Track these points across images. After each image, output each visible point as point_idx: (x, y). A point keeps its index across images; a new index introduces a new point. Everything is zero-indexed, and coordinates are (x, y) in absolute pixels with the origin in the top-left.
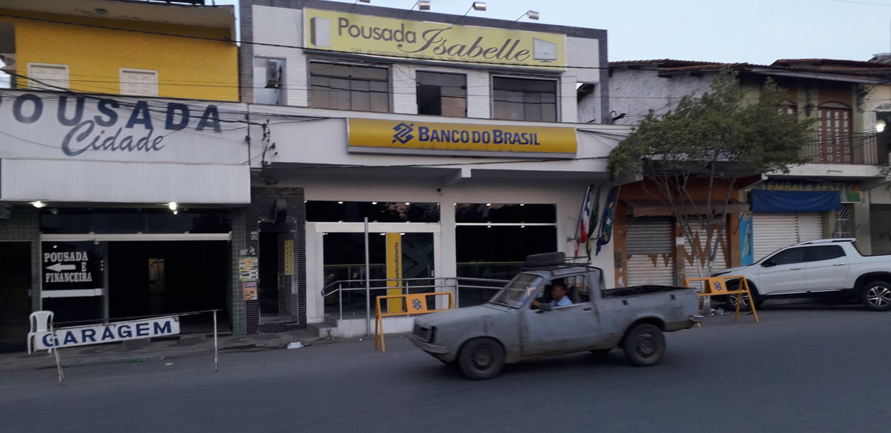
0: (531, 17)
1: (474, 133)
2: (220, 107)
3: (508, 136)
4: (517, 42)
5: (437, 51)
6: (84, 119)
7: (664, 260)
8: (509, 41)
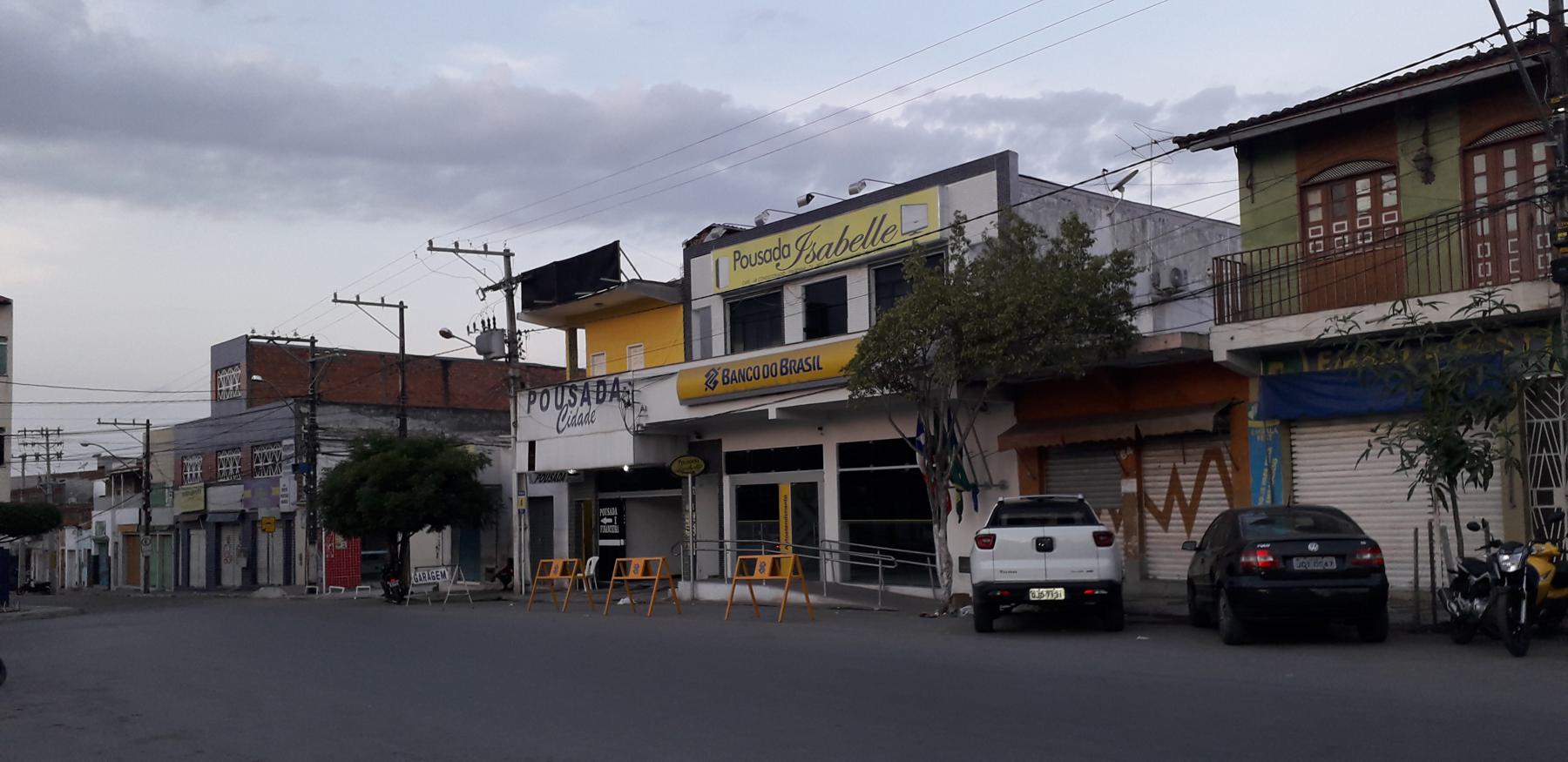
0: (851, 193)
1: (764, 366)
2: (621, 378)
3: (793, 364)
4: (884, 216)
5: (809, 260)
6: (564, 404)
7: (1113, 519)
8: (875, 219)
